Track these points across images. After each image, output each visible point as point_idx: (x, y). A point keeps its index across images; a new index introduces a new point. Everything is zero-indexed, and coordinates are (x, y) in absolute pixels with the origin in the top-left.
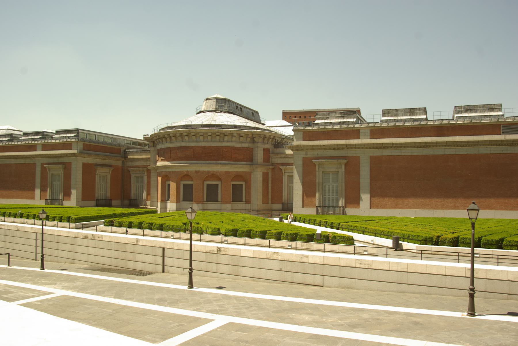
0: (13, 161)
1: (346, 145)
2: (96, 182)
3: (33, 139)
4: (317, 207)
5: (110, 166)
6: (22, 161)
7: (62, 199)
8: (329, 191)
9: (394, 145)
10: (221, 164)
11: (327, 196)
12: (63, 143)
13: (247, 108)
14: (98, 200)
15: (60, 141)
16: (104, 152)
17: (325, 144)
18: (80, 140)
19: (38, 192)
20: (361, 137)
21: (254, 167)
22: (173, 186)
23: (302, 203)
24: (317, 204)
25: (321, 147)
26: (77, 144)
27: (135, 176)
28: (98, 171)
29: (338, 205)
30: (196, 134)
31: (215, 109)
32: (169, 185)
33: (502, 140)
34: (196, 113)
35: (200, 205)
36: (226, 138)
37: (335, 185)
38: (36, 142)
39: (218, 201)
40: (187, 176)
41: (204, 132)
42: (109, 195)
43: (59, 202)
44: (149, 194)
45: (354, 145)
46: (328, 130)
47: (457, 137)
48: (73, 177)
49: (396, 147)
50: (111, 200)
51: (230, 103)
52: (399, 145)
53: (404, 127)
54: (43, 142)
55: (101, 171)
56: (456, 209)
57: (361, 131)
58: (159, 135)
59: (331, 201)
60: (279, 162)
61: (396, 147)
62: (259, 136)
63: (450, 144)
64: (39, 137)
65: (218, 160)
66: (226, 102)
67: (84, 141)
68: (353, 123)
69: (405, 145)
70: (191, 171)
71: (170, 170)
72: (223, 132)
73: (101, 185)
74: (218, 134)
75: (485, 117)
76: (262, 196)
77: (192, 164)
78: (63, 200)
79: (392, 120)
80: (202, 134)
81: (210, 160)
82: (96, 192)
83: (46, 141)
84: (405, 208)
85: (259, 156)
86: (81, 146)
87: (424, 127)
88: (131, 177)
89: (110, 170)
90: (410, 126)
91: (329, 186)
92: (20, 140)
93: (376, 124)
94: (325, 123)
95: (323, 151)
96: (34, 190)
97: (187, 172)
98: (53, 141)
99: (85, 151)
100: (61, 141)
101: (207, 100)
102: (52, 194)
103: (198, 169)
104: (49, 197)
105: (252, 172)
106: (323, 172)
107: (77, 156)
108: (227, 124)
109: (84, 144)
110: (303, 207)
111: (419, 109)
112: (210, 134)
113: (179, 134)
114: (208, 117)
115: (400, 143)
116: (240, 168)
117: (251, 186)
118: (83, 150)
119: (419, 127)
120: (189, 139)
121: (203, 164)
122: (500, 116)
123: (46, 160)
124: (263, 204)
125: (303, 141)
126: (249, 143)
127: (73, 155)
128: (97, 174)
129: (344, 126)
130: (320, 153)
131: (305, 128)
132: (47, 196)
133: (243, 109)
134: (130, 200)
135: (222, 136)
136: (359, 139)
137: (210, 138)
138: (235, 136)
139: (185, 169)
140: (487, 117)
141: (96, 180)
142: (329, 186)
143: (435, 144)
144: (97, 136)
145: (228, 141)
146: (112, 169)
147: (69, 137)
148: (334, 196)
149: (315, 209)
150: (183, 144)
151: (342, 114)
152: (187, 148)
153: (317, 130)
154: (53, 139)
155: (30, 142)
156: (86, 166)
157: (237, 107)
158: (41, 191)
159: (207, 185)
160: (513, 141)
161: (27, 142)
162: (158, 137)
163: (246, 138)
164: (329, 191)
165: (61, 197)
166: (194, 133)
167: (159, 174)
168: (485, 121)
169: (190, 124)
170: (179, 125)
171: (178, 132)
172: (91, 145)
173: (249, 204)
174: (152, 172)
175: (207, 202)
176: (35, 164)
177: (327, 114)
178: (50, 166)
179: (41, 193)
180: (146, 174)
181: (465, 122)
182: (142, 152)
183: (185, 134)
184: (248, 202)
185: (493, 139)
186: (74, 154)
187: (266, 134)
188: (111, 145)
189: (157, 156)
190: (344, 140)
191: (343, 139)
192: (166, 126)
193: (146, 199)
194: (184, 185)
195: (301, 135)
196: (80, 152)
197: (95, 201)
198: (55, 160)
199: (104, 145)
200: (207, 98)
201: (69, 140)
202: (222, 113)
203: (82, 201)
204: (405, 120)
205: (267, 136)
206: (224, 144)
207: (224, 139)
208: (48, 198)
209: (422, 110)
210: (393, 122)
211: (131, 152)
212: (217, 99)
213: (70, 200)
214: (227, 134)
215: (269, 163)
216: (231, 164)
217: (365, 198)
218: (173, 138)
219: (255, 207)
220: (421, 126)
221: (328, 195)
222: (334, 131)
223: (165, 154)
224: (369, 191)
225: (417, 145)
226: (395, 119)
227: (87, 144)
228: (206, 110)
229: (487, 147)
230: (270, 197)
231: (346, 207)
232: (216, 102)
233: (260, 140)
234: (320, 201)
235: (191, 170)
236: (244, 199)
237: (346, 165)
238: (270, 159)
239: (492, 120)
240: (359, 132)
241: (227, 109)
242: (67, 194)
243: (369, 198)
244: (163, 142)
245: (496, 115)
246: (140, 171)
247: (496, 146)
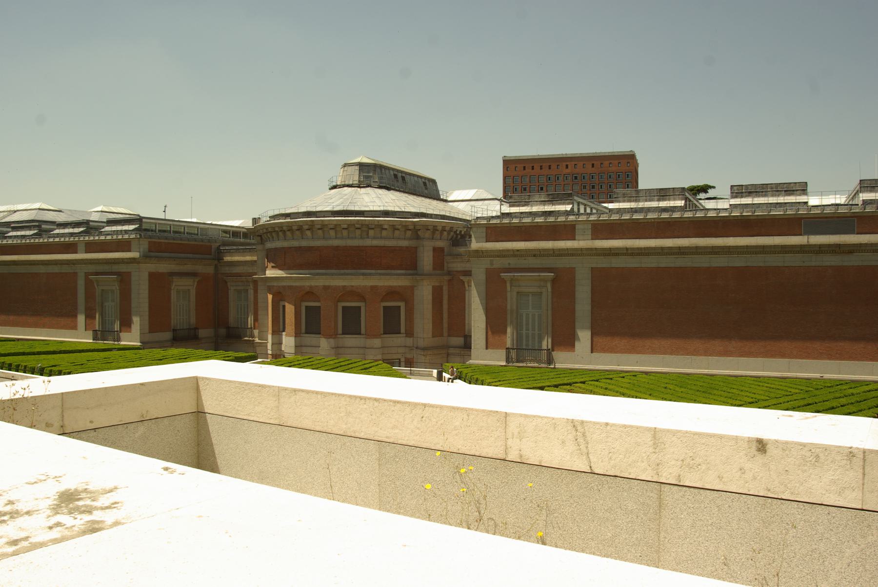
0: (42, 269)
1: (553, 249)
2: (172, 301)
3: (72, 234)
4: (507, 348)
5: (194, 274)
6: (56, 269)
7: (118, 330)
8: (527, 324)
9: (629, 252)
10: (363, 274)
11: (524, 332)
12: (117, 241)
13: (414, 175)
14: (176, 330)
15: (112, 237)
16: (185, 253)
17: (519, 249)
18: (143, 236)
19: (81, 319)
20: (577, 237)
21: (418, 278)
22: (290, 309)
23: (485, 343)
24: (509, 345)
25: (513, 252)
26: (139, 242)
27: (235, 290)
29: (541, 346)
30: (323, 226)
31: (357, 182)
32: (284, 307)
33: (801, 245)
34: (328, 187)
35: (332, 341)
36: (371, 232)
37: (537, 314)
38: (77, 239)
39: (360, 334)
40: (310, 294)
41: (335, 223)
42: (193, 320)
43: (114, 334)
44: (256, 320)
45: (565, 251)
46: (525, 225)
47: (731, 238)
48: (134, 295)
49: (633, 253)
50: (196, 329)
51: (383, 171)
52: (637, 252)
53: (646, 221)
54: (87, 238)
55: (179, 285)
56: (727, 356)
57: (577, 227)
58: (267, 227)
59: (530, 338)
60: (459, 269)
61: (632, 254)
62: (426, 227)
63: (719, 250)
64: (81, 229)
65: (359, 269)
66: (375, 170)
67: (150, 237)
68: (567, 213)
69: (646, 251)
70: (317, 286)
71: (284, 284)
72: (367, 223)
73: (180, 305)
74: (357, 226)
75: (777, 206)
76: (431, 325)
77: (318, 274)
78: (120, 332)
79: (626, 209)
80: (332, 226)
82: (172, 316)
83: (92, 238)
84: (646, 353)
85: (426, 259)
86: (145, 245)
87: (679, 221)
88: (229, 290)
90: (656, 220)
91: (527, 315)
92: (52, 236)
93: (601, 215)
94: (522, 213)
95: (518, 258)
96: (76, 316)
97: (311, 287)
98: (102, 238)
99: (152, 254)
100: (115, 237)
101: (345, 166)
102: (103, 322)
103: (327, 284)
104: (99, 326)
105: (415, 286)
106: (518, 293)
107: (139, 263)
108: (372, 209)
110: (487, 348)
111: (674, 190)
112: (345, 226)
113: (296, 227)
114: (345, 198)
115: (641, 249)
116: (397, 281)
117: (414, 309)
119: (669, 222)
120: (312, 235)
121: (336, 274)
122: (800, 204)
123: (91, 268)
124: (433, 337)
125: (486, 242)
126: (410, 239)
127: (132, 261)
129: (551, 219)
130: (513, 262)
131: (489, 221)
132: (95, 325)
133: (407, 178)
134: (228, 328)
135: (365, 229)
136: (575, 240)
137: (345, 233)
138: (386, 229)
139: (307, 284)
140: (781, 205)
141: (172, 298)
142: (527, 315)
143: (694, 251)
144: (172, 227)
145: (374, 238)
146: (197, 280)
147: (126, 232)
148: (535, 331)
149: (503, 353)
150: (304, 243)
151: (551, 197)
152: (310, 249)
153: (509, 225)
154: (103, 233)
155: (67, 239)
156: (153, 276)
157: (396, 176)
158: (86, 318)
159: (344, 308)
160: (820, 248)
161: (62, 239)
162: (265, 231)
163: (405, 232)
164: (527, 324)
165: (117, 327)
166: (320, 226)
167: (270, 290)
168: (776, 212)
169: (314, 210)
170: (296, 211)
171: (294, 224)
172: (161, 242)
173: (410, 337)
174: (259, 284)
175: (343, 336)
176: (75, 274)
177: (527, 197)
178: (99, 278)
179: (87, 321)
180: (251, 287)
181: (744, 214)
182: (244, 252)
183: (306, 227)
184: (410, 334)
185: (787, 244)
186: (134, 259)
187: (437, 225)
188: (196, 241)
189: (266, 260)
190: (551, 242)
191: (550, 240)
192: (277, 212)
193: (252, 327)
194: (307, 307)
195: (482, 232)
196: (144, 256)
197: (171, 331)
198: (106, 268)
199: (183, 242)
200: (345, 164)
201: (126, 236)
202: (368, 189)
204: (649, 210)
205: (440, 228)
206: (368, 242)
207: (368, 234)
208: (97, 329)
209: (679, 192)
210: (629, 212)
211: (229, 251)
212: (361, 165)
213: (130, 332)
214: (373, 226)
215: (444, 270)
216: (380, 274)
217: (584, 336)
218: (288, 233)
219: (421, 343)
220: (673, 220)
221: (526, 330)
222: (535, 226)
223: (278, 258)
224: (589, 325)
225: (665, 251)
226: (632, 208)
227: (154, 242)
228: (343, 183)
229: (779, 255)
230: (445, 325)
231: (553, 350)
232: (359, 170)
233: (428, 234)
234: (513, 340)
235: (317, 284)
236: (403, 330)
237: (554, 281)
238: (446, 264)
239: (788, 211)
240: (575, 228)
241: (377, 182)
242: (126, 324)
243: (590, 337)
244: (273, 238)
245: (795, 203)
246: (242, 281)
247: (793, 255)
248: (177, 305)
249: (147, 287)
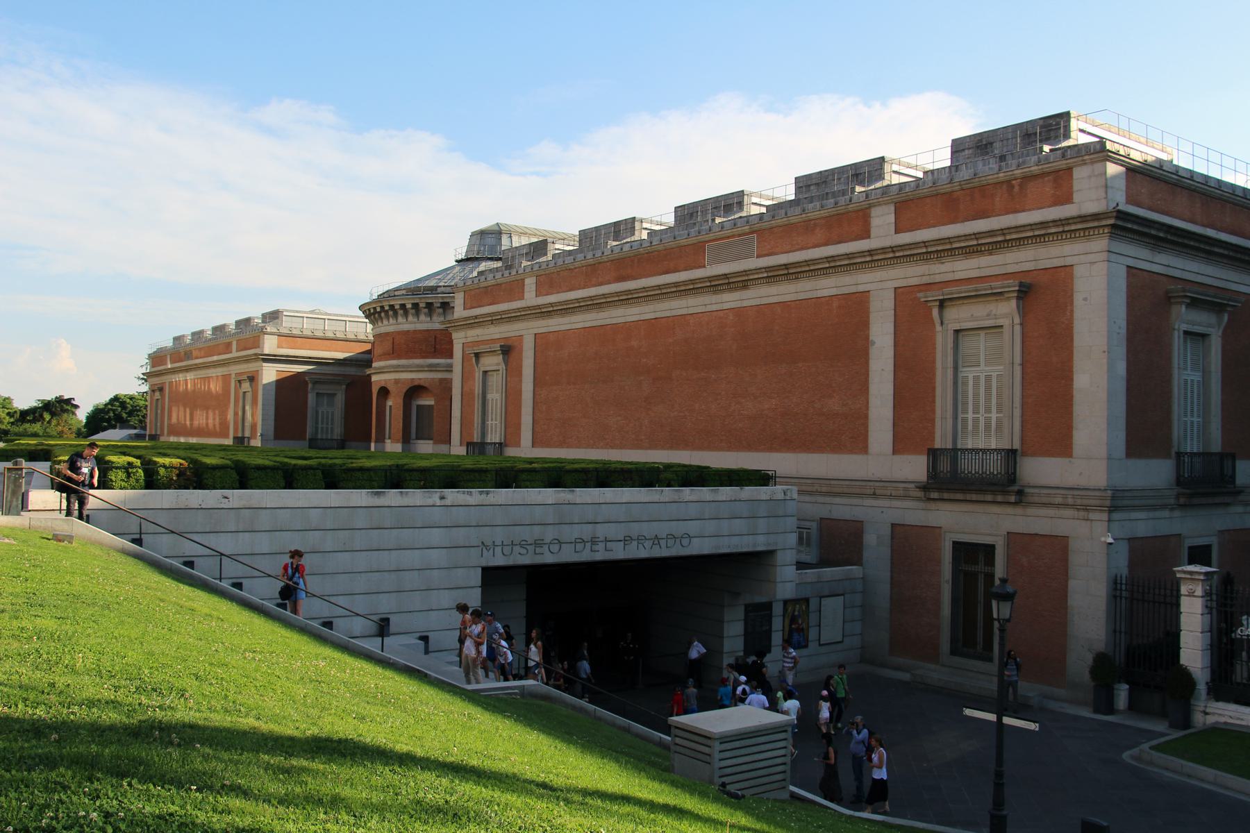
8: (492, 413)
81: (416, 358)
118: (278, 347)
152: (387, 334)
164: (492, 413)
175: (416, 441)
248: (317, 412)
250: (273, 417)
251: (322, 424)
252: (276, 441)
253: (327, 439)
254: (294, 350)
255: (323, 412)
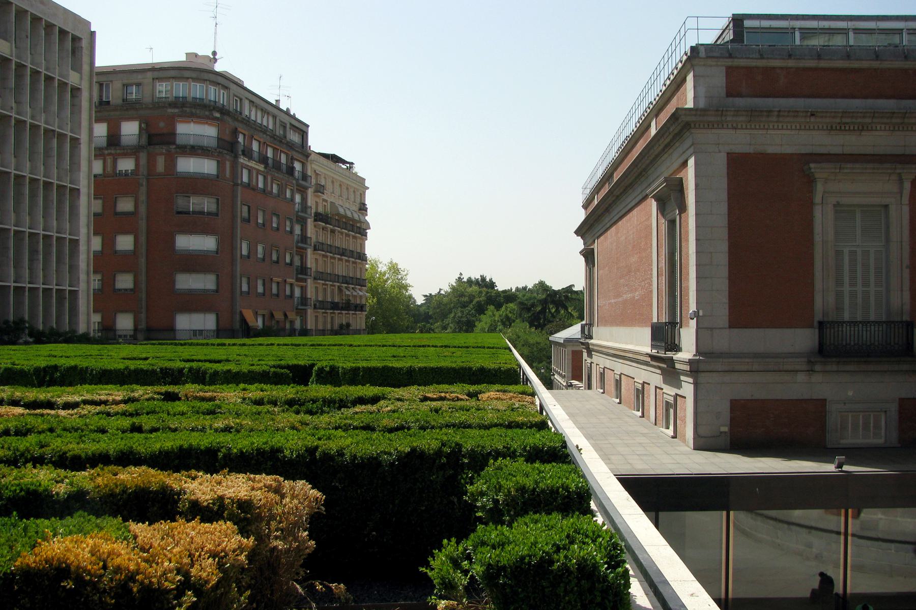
2: (818, 238)
28: (820, 188)
89: (901, 181)
99: (741, 102)
109: (730, 71)
128: (818, 199)
141: (818, 229)
172: (774, 68)
203: (731, 326)
248: (839, 254)
249: (724, 196)
250: (724, 272)
251: (853, 284)
252: (732, 330)
253: (866, 323)
254: (771, 100)
255: (853, 253)
